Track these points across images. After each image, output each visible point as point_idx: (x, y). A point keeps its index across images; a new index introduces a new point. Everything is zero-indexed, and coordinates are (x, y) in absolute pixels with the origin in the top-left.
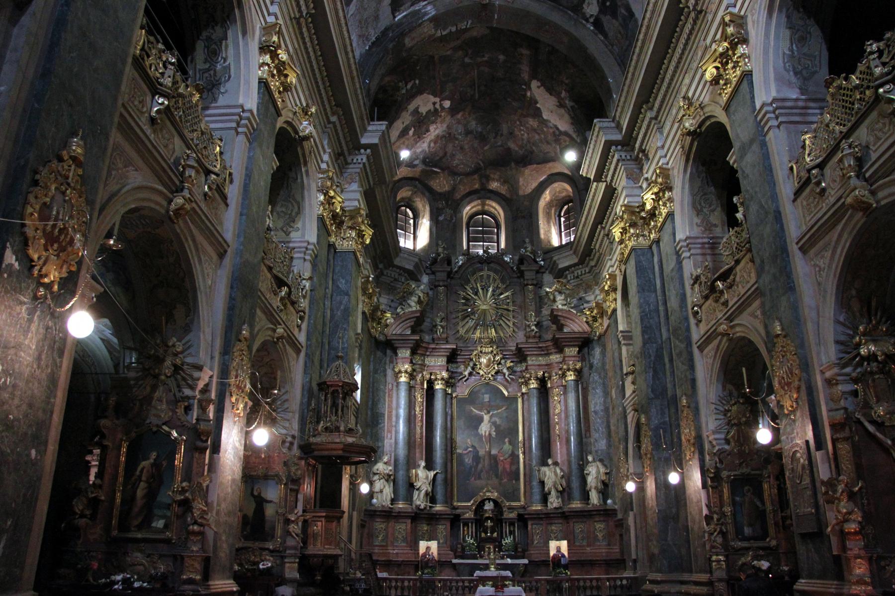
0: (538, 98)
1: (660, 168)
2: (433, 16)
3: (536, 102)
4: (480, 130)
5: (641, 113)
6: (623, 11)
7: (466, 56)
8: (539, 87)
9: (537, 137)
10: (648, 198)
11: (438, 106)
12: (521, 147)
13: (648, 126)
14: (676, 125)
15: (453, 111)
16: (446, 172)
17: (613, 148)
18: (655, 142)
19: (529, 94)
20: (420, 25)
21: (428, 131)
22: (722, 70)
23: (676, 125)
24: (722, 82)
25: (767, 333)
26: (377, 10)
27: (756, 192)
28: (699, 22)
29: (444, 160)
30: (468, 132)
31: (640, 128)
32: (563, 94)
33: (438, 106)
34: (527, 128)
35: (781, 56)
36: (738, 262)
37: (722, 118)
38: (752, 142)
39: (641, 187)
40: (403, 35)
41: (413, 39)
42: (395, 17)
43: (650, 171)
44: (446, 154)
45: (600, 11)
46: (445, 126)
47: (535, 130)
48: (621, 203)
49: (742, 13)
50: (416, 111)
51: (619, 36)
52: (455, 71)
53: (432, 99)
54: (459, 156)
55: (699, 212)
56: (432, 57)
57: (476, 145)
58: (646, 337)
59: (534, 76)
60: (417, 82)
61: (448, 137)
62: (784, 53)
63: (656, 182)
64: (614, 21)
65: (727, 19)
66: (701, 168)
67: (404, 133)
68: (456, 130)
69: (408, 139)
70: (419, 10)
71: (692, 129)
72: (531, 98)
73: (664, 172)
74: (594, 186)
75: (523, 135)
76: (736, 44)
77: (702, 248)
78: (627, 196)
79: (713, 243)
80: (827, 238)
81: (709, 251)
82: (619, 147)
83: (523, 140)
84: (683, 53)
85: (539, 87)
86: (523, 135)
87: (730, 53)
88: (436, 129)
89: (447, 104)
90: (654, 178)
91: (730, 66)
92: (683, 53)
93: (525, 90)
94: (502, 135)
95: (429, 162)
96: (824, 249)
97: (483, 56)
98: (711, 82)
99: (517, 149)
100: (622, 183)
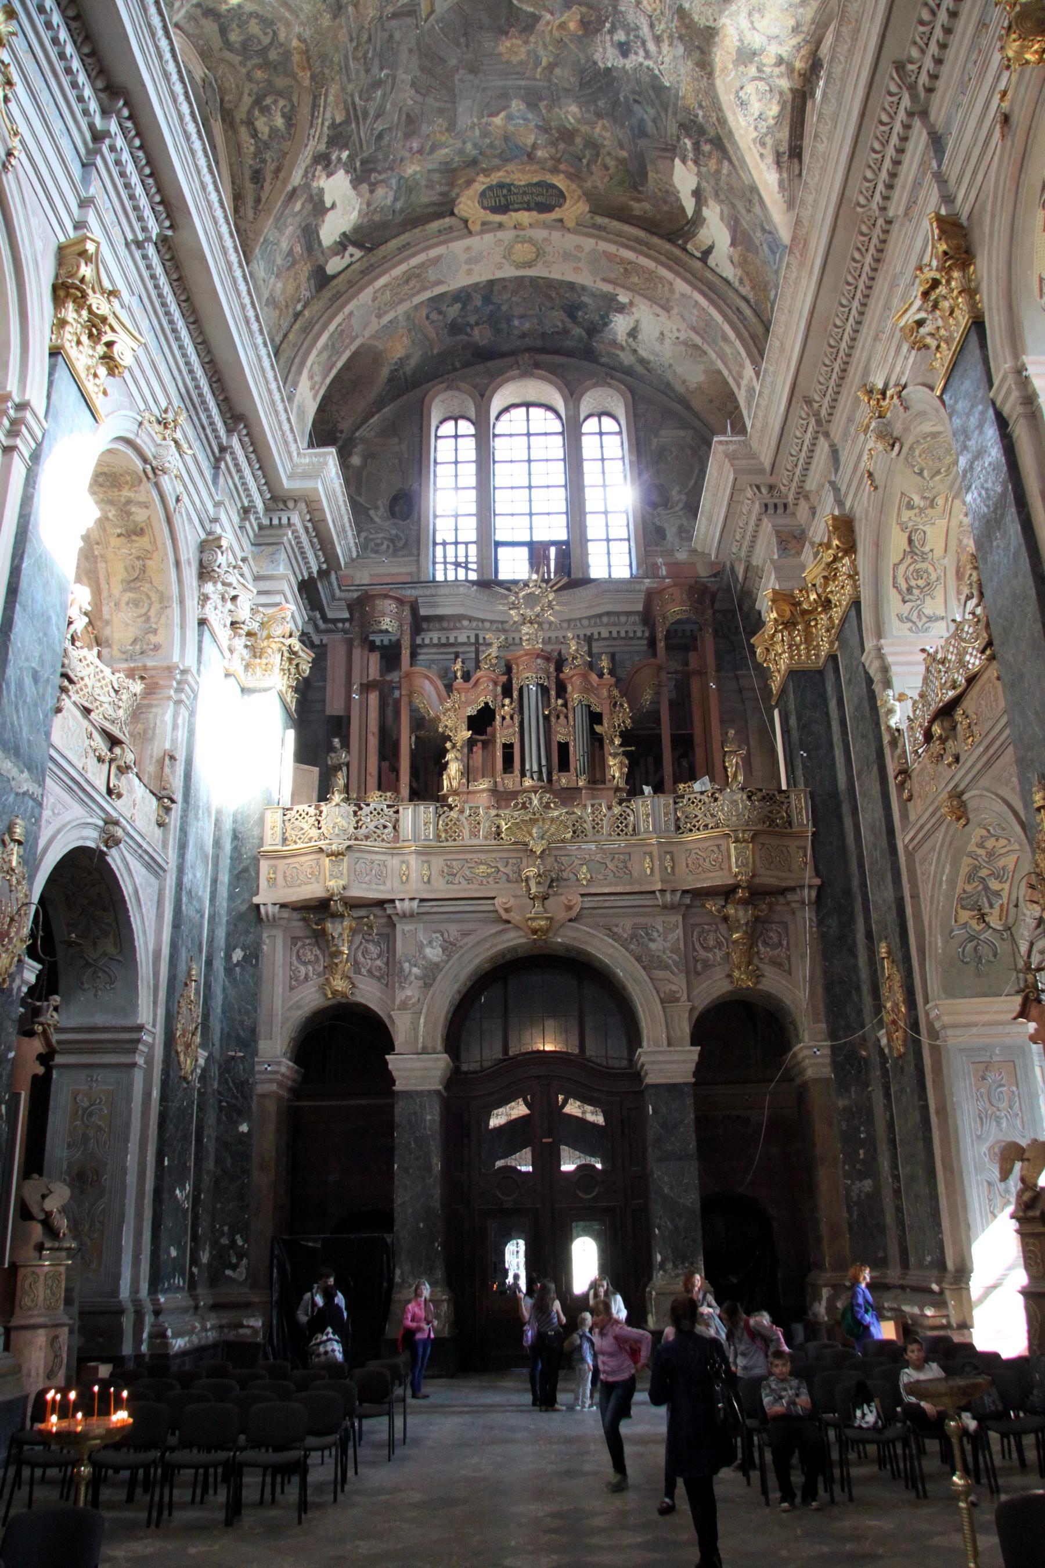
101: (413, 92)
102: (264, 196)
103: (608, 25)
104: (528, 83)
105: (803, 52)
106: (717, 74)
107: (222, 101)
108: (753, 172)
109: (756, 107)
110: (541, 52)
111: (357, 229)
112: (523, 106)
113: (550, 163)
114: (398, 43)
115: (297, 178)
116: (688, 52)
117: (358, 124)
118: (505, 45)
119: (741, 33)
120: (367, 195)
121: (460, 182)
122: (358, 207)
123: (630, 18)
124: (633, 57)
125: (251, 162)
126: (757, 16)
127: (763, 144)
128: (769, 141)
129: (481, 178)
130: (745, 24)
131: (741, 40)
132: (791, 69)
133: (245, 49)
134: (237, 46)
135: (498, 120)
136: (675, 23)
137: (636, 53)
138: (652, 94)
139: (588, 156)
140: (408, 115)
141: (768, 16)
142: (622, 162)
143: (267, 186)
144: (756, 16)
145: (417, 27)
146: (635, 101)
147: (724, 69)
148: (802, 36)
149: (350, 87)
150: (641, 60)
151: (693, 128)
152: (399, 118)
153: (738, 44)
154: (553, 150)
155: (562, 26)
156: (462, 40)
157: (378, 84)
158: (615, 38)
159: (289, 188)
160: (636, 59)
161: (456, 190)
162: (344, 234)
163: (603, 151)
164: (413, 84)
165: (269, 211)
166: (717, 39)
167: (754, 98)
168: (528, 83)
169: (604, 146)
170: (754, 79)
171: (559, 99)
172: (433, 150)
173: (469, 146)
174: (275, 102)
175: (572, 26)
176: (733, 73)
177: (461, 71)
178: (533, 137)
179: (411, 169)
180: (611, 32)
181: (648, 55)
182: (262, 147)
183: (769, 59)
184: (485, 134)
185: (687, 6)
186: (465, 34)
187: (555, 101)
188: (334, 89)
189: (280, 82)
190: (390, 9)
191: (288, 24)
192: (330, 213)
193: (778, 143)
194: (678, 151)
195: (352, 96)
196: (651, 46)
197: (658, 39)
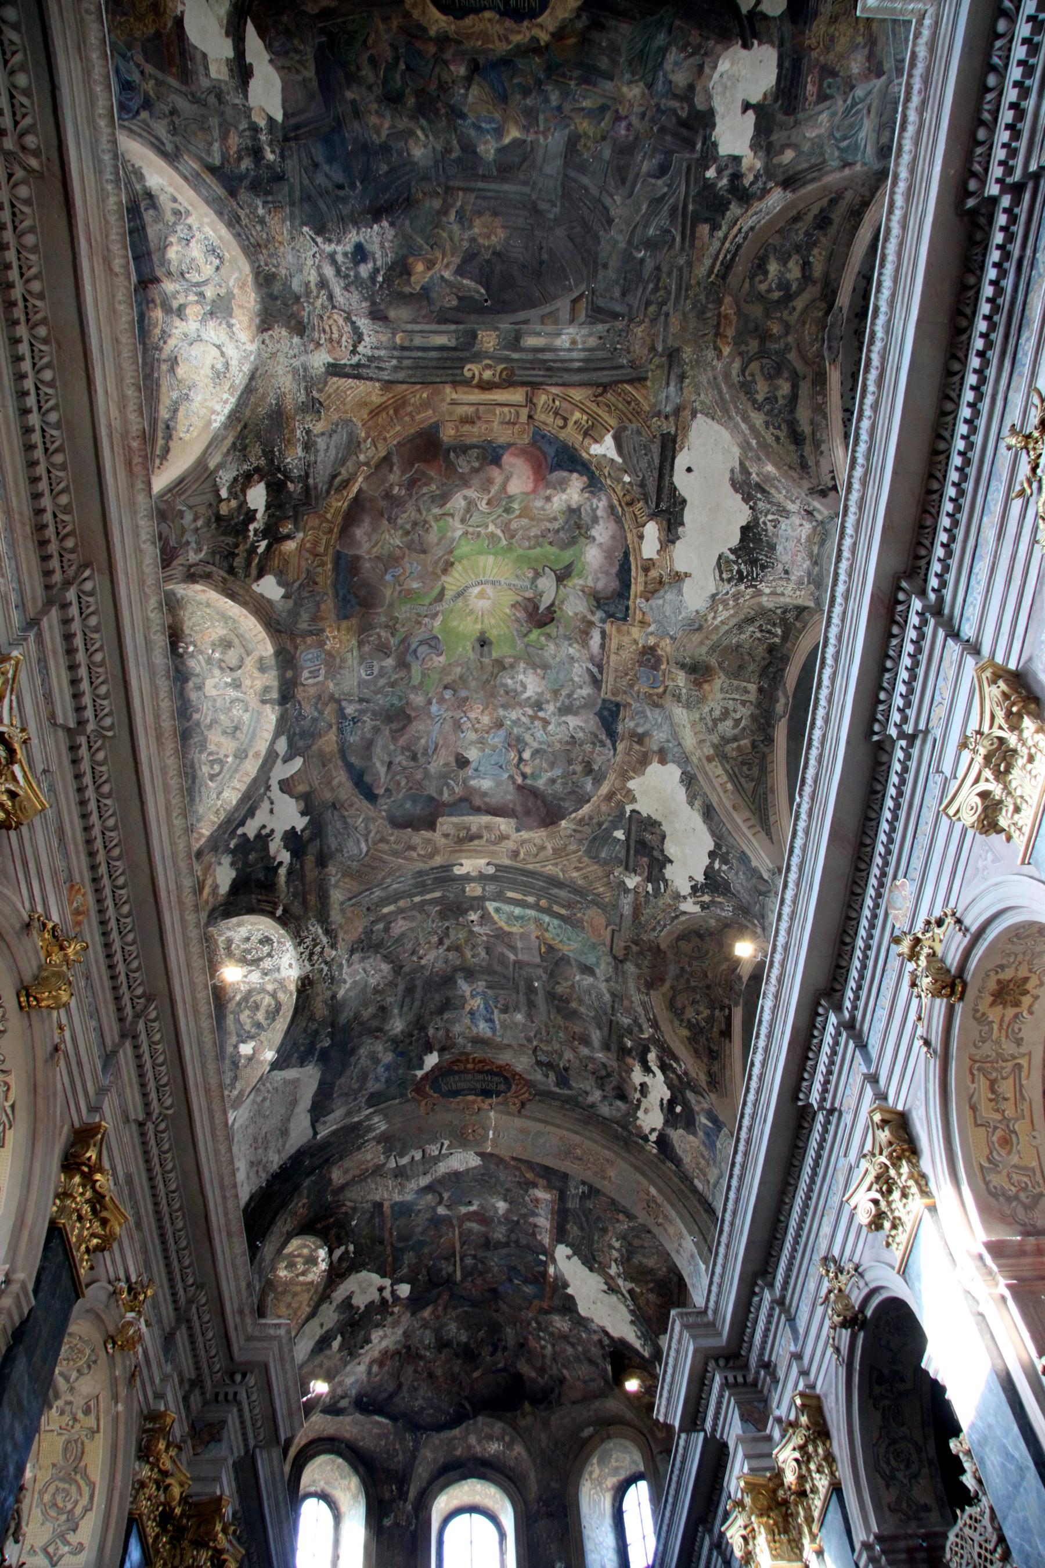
0: (568, 1277)
1: (802, 1395)
2: (383, 1133)
3: (566, 1285)
4: (464, 1338)
5: (755, 1294)
6: (704, 1120)
7: (440, 1203)
8: (569, 1257)
9: (570, 1350)
10: (786, 1456)
11: (387, 1294)
12: (542, 1371)
13: (770, 1316)
14: (820, 1310)
15: (415, 1303)
16: (400, 1424)
18: (784, 1347)
19: (551, 1270)
20: (359, 1148)
21: (367, 1341)
22: (883, 1204)
23: (820, 1310)
24: (887, 1225)
26: (287, 1120)
28: (832, 1128)
29: (397, 1399)
30: (442, 1344)
31: (755, 1322)
32: (613, 1270)
33: (387, 1294)
34: (552, 1334)
35: (977, 1170)
37: (898, 1288)
39: (769, 1438)
40: (328, 1162)
41: (346, 1172)
42: (316, 1133)
43: (785, 1402)
44: (400, 1386)
45: (667, 1122)
46: (400, 1331)
47: (564, 1337)
48: (736, 1472)
49: (900, 1108)
50: (347, 1304)
52: (419, 1229)
53: (376, 1279)
54: (424, 1391)
56: (379, 1205)
57: (457, 1369)
59: (561, 1235)
60: (351, 1248)
61: (406, 1353)
62: (982, 1167)
63: (794, 1425)
64: (691, 1138)
65: (877, 1117)
66: (877, 1390)
67: (323, 1343)
68: (421, 1341)
69: (329, 1358)
70: (360, 1123)
71: (849, 1314)
72: (556, 1278)
73: (813, 1405)
74: (682, 1443)
75: (543, 1348)
76: (899, 1158)
78: (747, 1457)
82: (722, 1362)
83: (544, 1357)
84: (813, 1181)
85: (569, 1257)
86: (543, 1348)
87: (892, 1172)
88: (382, 1338)
89: (404, 1290)
90: (792, 1417)
91: (896, 1195)
92: (813, 1181)
93: (545, 1264)
94: (505, 1349)
95: (368, 1404)
97: (470, 1203)
98: (870, 1225)
99: (533, 1374)
100: (734, 1430)
101: (612, 212)
102: (824, 202)
103: (380, 279)
104: (472, 185)
105: (157, 331)
106: (250, 279)
107: (827, 314)
108: (180, 181)
109: (196, 251)
110: (455, 228)
111: (725, 37)
112: (481, 149)
113: (448, 55)
114: (617, 282)
115: (776, 200)
116: (286, 285)
117: (685, 207)
118: (498, 237)
119: (232, 336)
120: (698, 88)
121: (572, 41)
122: (716, 76)
123: (355, 297)
124: (349, 248)
125: (823, 240)
126: (219, 366)
127: (177, 213)
128: (170, 218)
129: (544, 37)
130: (231, 351)
131: (230, 326)
132: (168, 310)
133: (778, 368)
134: (786, 375)
135: (513, 133)
136: (305, 314)
137: (345, 254)
138: (323, 207)
139: (398, 77)
140: (623, 181)
141: (209, 372)
142: (352, 79)
143: (815, 210)
144: (219, 366)
145: (593, 292)
146: (341, 187)
147: (242, 287)
148: (164, 356)
149: (681, 261)
150: (339, 249)
151: (266, 183)
152: (634, 184)
153: (233, 321)
154: (445, 77)
155: (430, 264)
156: (545, 256)
157: (651, 245)
158: (370, 266)
159: (789, 195)
160: (342, 249)
161: (580, 25)
162: (746, 46)
163: (378, 91)
164: (610, 221)
165: (824, 188)
166: (257, 321)
167: (201, 260)
168: (472, 185)
169: (379, 101)
170: (205, 283)
171: (436, 162)
172: (603, 109)
173: (554, 98)
174: (769, 291)
175: (420, 267)
176: (231, 283)
177: (551, 216)
178: (470, 99)
179: (633, 92)
180: (376, 271)
181: (332, 257)
182: (803, 250)
183: (194, 311)
184: (531, 115)
185: (296, 340)
186: (541, 263)
187: (441, 158)
188: (701, 271)
189: (756, 311)
190: (619, 325)
191: (727, 375)
192: (755, 98)
193: (159, 218)
194: (280, 135)
195: (682, 249)
196: (329, 271)
197: (323, 284)
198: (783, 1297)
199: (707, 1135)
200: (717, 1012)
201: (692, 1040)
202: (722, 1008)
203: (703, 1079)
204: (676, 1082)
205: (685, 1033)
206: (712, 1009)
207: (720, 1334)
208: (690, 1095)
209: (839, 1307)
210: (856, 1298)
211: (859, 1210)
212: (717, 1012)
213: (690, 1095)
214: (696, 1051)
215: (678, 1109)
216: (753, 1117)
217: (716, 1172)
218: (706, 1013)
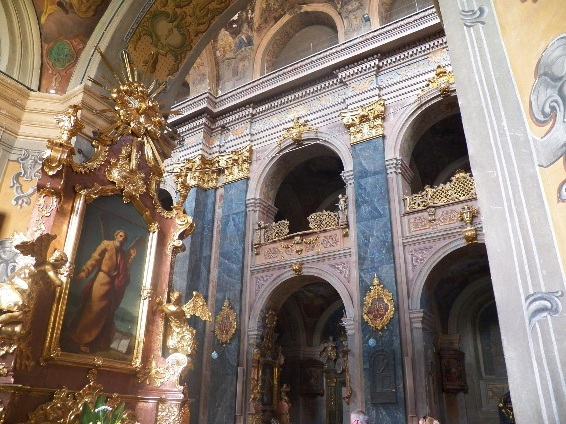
6: (244, 37)
17: (206, 115)
25: (361, 281)
27: (372, 200)
36: (325, 231)
38: (376, 173)
51: (228, 48)
55: (267, 186)
58: (192, 249)
64: (231, 38)
77: (264, 209)
79: (269, 209)
80: (429, 245)
81: (265, 212)
82: (208, 116)
96: (426, 249)
198: (255, 115)
199: (241, 43)
200: (280, 10)
201: (264, 11)
202: (283, 10)
203: (256, 25)
204: (244, 17)
205: (264, 6)
206: (280, 8)
207: (215, 108)
208: (245, 26)
209: (299, 135)
210: (304, 136)
211: (345, 119)
212: (280, 10)
213: (245, 26)
214: (262, 15)
215: (235, 26)
216: (312, 62)
217: (232, 55)
218: (276, 7)
